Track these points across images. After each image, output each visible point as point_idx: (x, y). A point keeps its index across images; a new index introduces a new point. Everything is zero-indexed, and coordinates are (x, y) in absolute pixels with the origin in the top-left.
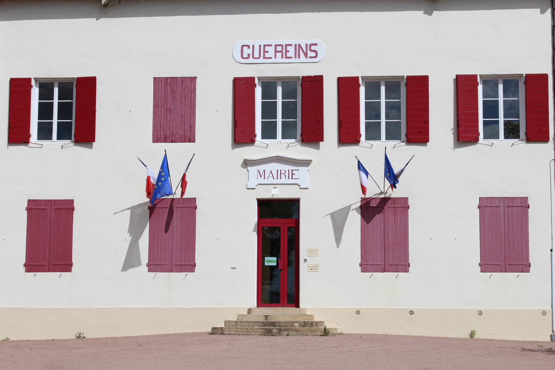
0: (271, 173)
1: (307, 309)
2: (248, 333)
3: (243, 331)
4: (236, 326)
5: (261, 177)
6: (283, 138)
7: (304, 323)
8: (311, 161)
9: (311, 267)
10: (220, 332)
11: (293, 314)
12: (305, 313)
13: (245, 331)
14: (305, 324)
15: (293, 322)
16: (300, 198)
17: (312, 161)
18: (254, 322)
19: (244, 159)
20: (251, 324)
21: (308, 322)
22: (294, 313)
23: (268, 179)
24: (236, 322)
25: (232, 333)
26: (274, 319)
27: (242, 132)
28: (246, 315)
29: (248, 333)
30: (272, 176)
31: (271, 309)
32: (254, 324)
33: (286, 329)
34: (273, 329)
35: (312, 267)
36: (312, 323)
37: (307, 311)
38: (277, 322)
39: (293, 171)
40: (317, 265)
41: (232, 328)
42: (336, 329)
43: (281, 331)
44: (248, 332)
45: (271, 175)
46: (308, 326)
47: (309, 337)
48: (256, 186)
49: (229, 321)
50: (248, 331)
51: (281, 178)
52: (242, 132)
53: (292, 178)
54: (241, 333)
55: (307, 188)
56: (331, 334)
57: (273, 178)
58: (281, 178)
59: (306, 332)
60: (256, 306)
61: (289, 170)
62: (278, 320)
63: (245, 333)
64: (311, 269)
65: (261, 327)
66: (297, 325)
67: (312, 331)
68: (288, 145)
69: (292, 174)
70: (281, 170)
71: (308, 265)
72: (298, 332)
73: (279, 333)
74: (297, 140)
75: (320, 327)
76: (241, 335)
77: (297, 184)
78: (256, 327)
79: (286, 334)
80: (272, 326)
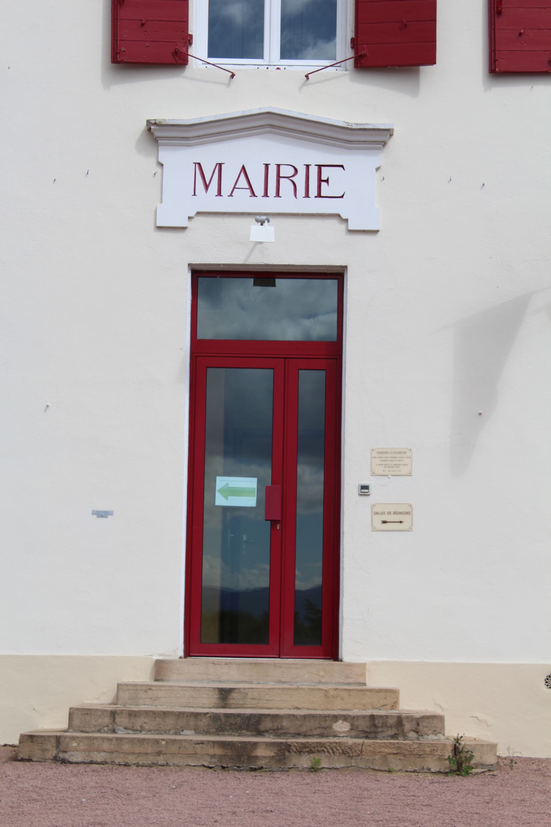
0: (242, 175)
1: (367, 667)
2: (161, 760)
3: (141, 750)
4: (114, 731)
5: (207, 187)
6: (283, 56)
7: (368, 723)
8: (389, 132)
9: (383, 513)
10: (53, 752)
11: (320, 682)
12: (362, 681)
13: (150, 750)
14: (375, 726)
15: (328, 716)
16: (346, 267)
17: (391, 135)
18: (180, 715)
19: (148, 121)
20: (170, 721)
21: (387, 717)
22: (323, 680)
23: (231, 195)
24: (113, 714)
25: (99, 757)
26: (254, 702)
27: (143, 24)
28: (148, 688)
29: (161, 760)
30: (247, 186)
31: (239, 664)
32: (182, 722)
33: (305, 745)
34: (255, 744)
35: (389, 513)
36: (400, 720)
37: (367, 673)
38: (269, 715)
39: (323, 168)
40: (408, 509)
41: (97, 738)
42: (493, 747)
43: (287, 753)
44: (162, 757)
45: (243, 182)
46: (384, 734)
47: (400, 779)
48: (190, 218)
49: (87, 712)
50: (159, 753)
51: (278, 194)
52: (143, 24)
53: (319, 195)
54: (132, 759)
55: (376, 232)
56: (477, 766)
57: (249, 191)
58: (278, 194)
59: (385, 757)
60: (181, 653)
61: (308, 166)
62: (268, 706)
63: (150, 760)
64: (384, 522)
65: (208, 733)
66: (341, 727)
67: (405, 756)
68: (307, 76)
69: (320, 181)
70: (278, 166)
71: (373, 506)
72: (351, 757)
73: (279, 761)
74: (332, 62)
75: (432, 738)
76: (135, 767)
77: (338, 216)
78: (189, 735)
79: (305, 766)
80: (247, 730)
